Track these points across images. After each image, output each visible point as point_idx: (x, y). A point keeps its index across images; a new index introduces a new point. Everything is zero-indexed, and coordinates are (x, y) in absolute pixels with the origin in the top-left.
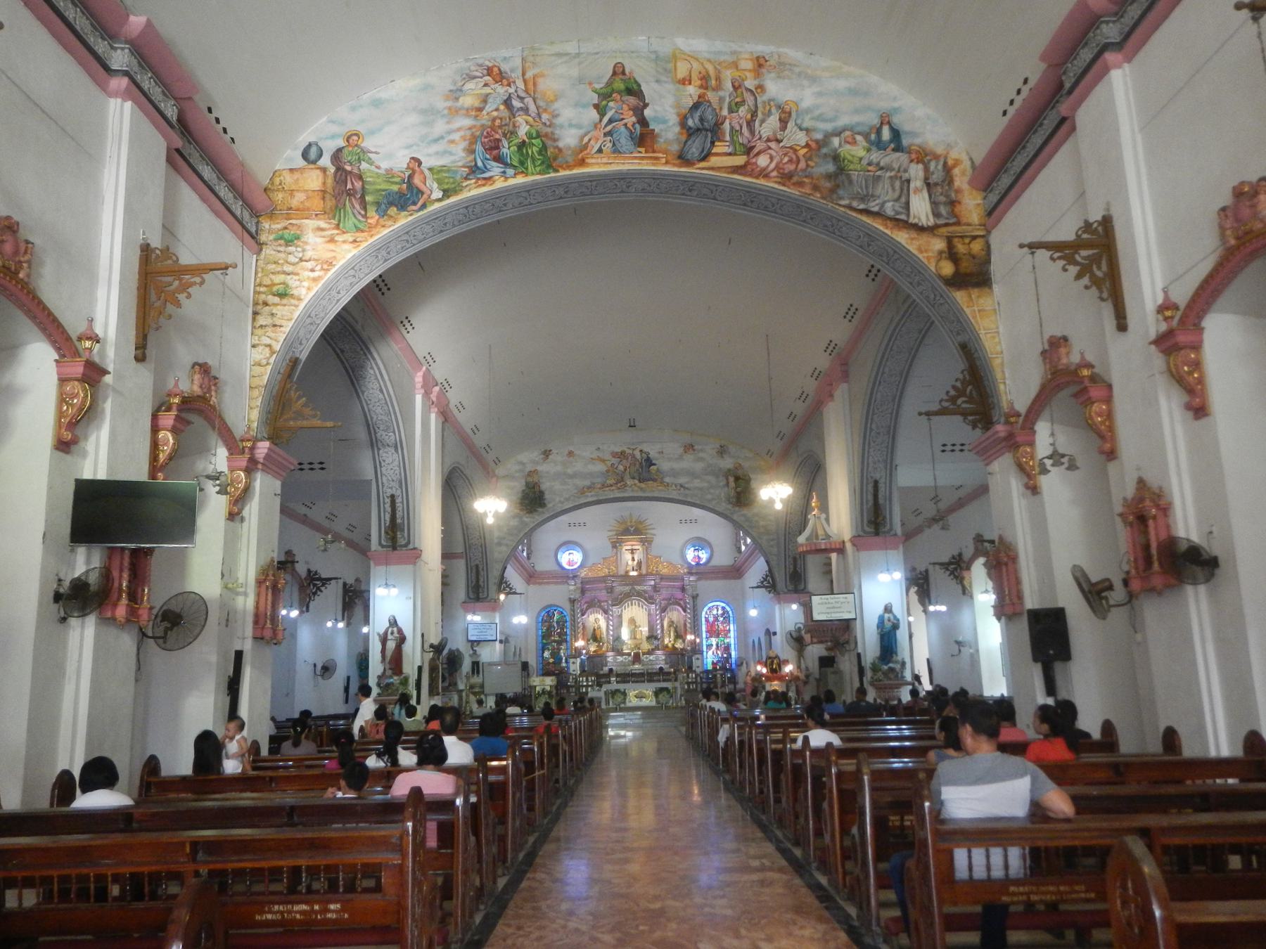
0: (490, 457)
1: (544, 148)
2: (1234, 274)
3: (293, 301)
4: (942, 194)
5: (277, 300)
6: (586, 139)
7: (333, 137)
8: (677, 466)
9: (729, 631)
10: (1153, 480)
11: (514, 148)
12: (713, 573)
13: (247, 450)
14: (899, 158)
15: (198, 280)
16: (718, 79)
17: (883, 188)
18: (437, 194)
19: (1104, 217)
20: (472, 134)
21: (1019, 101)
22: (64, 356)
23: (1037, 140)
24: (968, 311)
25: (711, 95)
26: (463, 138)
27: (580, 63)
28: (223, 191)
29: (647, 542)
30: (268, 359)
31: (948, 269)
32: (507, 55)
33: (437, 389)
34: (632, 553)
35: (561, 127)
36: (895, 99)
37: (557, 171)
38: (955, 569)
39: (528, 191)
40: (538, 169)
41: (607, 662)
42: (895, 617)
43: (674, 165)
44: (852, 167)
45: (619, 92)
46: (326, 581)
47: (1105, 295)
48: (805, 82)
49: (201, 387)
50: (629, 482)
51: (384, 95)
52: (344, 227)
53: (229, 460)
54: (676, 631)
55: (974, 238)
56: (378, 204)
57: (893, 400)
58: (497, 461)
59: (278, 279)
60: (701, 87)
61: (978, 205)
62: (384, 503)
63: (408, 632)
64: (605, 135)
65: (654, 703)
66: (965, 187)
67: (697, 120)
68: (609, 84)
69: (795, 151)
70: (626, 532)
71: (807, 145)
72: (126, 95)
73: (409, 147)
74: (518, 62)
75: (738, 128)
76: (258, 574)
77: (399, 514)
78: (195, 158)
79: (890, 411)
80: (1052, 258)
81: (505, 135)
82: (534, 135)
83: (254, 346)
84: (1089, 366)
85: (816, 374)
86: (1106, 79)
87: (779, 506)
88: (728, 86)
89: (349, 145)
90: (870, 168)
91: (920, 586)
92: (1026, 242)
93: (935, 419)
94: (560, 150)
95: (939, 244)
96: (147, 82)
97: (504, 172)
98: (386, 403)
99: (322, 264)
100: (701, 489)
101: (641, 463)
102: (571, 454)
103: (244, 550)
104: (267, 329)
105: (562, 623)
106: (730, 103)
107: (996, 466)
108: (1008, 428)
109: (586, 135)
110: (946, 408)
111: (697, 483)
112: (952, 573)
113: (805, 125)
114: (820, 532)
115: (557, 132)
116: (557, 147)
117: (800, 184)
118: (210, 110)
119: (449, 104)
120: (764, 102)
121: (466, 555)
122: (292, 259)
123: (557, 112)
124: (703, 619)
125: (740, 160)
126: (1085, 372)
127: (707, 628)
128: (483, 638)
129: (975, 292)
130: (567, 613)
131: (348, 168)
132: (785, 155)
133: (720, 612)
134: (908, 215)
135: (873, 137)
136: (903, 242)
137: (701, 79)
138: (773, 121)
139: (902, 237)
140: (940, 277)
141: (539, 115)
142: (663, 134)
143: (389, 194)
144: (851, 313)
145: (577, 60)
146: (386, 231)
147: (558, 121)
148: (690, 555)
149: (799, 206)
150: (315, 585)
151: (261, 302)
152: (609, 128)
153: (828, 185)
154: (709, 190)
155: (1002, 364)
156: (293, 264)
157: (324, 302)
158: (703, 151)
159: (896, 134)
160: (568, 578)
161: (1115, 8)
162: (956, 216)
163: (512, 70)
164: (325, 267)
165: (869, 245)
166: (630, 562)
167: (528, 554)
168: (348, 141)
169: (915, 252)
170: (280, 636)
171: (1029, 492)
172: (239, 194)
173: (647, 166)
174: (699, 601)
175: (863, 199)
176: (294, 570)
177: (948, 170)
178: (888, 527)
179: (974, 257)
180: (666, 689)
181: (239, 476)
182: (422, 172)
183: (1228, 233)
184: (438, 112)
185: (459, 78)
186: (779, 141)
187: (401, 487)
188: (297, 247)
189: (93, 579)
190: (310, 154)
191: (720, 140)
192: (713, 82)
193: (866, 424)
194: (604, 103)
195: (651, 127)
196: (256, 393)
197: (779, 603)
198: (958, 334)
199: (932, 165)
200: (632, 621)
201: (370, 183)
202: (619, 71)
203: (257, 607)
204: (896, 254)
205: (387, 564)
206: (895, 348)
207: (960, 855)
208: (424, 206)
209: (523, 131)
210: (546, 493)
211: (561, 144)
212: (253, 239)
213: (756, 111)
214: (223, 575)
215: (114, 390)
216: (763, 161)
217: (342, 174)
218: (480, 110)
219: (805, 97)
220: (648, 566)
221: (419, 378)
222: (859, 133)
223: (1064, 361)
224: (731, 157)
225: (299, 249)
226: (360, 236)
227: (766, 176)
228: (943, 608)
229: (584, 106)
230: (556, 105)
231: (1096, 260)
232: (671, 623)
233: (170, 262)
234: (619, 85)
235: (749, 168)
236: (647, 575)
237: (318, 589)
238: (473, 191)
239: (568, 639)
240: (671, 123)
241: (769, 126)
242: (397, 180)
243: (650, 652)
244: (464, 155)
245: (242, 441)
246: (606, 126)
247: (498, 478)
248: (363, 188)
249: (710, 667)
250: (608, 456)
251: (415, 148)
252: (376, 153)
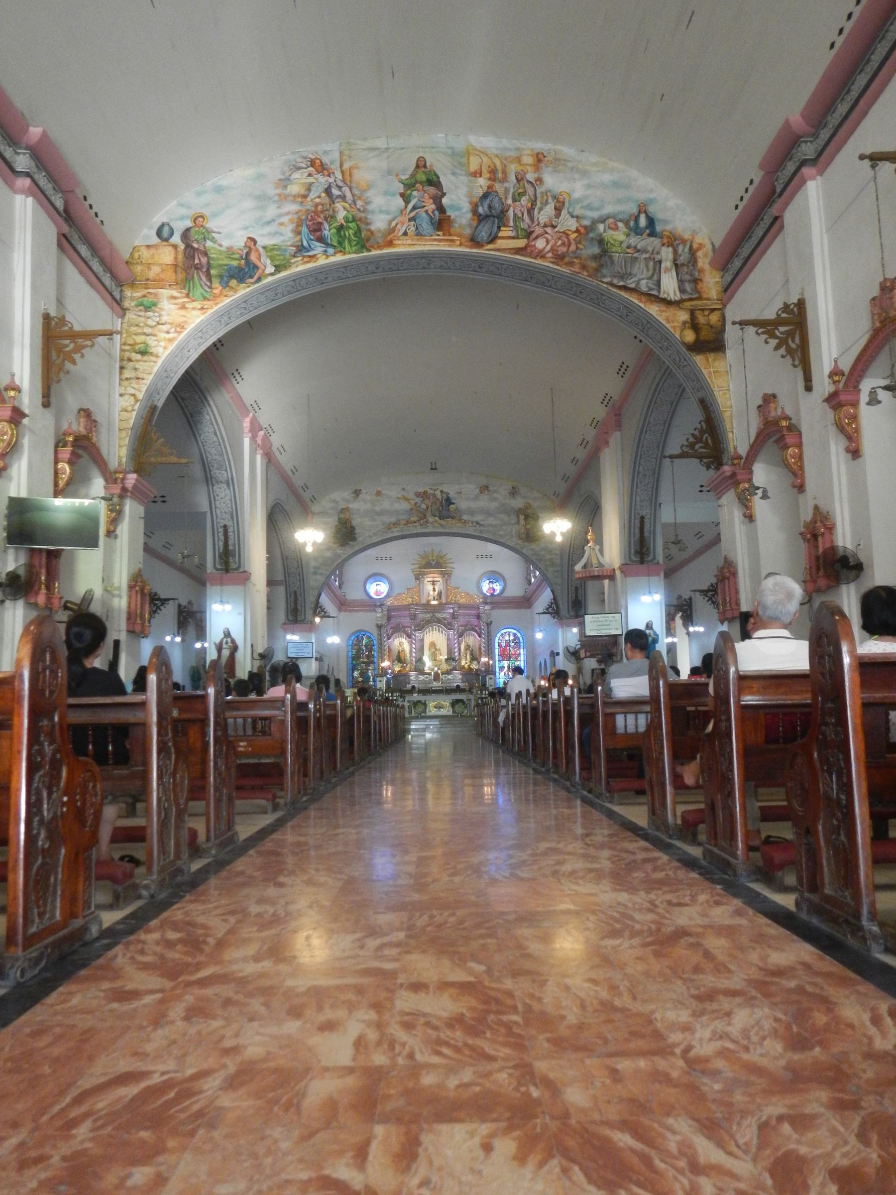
0: (306, 496)
1: (359, 231)
2: (880, 348)
3: (153, 358)
4: (687, 273)
5: (139, 357)
6: (394, 224)
7: (182, 218)
8: (473, 505)
9: (519, 654)
10: (823, 507)
11: (334, 231)
12: (506, 603)
13: (119, 481)
14: (653, 242)
15: (89, 343)
16: (504, 172)
17: (639, 268)
18: (270, 269)
19: (799, 300)
20: (299, 219)
21: (747, 197)
23: (759, 232)
24: (704, 371)
25: (498, 187)
26: (291, 221)
27: (388, 157)
28: (96, 265)
29: (447, 575)
30: (133, 406)
31: (690, 336)
32: (327, 148)
33: (261, 433)
34: (433, 584)
35: (373, 212)
36: (651, 191)
37: (370, 251)
38: (713, 595)
39: (345, 267)
40: (354, 249)
41: (410, 680)
42: (655, 633)
43: (467, 247)
44: (614, 249)
45: (421, 183)
46: (164, 601)
47: (797, 362)
48: (577, 176)
49: (85, 428)
50: (431, 519)
51: (224, 181)
53: (105, 488)
54: (472, 654)
55: (713, 310)
56: (221, 277)
57: (658, 446)
58: (313, 499)
60: (490, 179)
61: (717, 282)
63: (240, 642)
64: (410, 220)
65: (451, 713)
66: (707, 267)
67: (486, 206)
68: (413, 175)
69: (567, 235)
70: (428, 565)
71: (577, 231)
72: (28, 192)
73: (246, 228)
74: (336, 155)
75: (520, 215)
76: (130, 581)
77: (231, 542)
79: (655, 456)
80: (757, 333)
81: (326, 219)
82: (351, 219)
83: (121, 395)
84: (788, 418)
85: (595, 423)
86: (803, 188)
87: (559, 539)
88: (513, 178)
89: (196, 226)
90: (629, 251)
91: (684, 611)
92: (737, 320)
93: (676, 461)
94: (372, 233)
95: (684, 316)
96: (43, 182)
97: (325, 251)
98: (220, 445)
100: (494, 526)
101: (441, 503)
102: (379, 493)
103: (118, 560)
105: (370, 647)
106: (513, 193)
107: (724, 500)
108: (732, 468)
109: (393, 219)
110: (687, 452)
111: (491, 521)
112: (710, 599)
113: (575, 214)
114: (594, 561)
115: (369, 217)
116: (370, 230)
117: (571, 264)
118: (85, 198)
119: (278, 191)
120: (542, 193)
121: (286, 583)
123: (369, 200)
124: (497, 645)
125: (521, 243)
126: (784, 423)
127: (500, 652)
128: (300, 655)
129: (711, 356)
130: (375, 638)
131: (195, 245)
132: (559, 238)
133: (512, 638)
134: (659, 291)
135: (632, 223)
136: (654, 314)
137: (490, 172)
138: (549, 209)
139: (653, 310)
140: (684, 343)
141: (354, 202)
142: (458, 219)
143: (230, 268)
144: (623, 370)
145: (386, 155)
146: (228, 300)
147: (370, 207)
148: (486, 586)
149: (570, 282)
150: (155, 605)
151: (126, 358)
152: (412, 214)
153: (593, 264)
154: (496, 267)
155: (731, 416)
157: (177, 359)
158: (491, 234)
159: (651, 221)
160: (375, 606)
161: (813, 130)
162: (698, 292)
163: (332, 162)
164: (178, 329)
165: (627, 316)
166: (431, 593)
167: (340, 584)
168: (195, 221)
169: (664, 322)
170: (146, 632)
171: (747, 520)
172: (108, 269)
173: (444, 247)
174: (493, 627)
175: (622, 277)
177: (693, 252)
178: (651, 556)
179: (712, 327)
180: (462, 701)
182: (257, 250)
183: (876, 317)
184: (270, 198)
185: (286, 169)
186: (554, 227)
187: (232, 518)
188: (155, 312)
189: (22, 572)
190: (163, 233)
191: (505, 226)
192: (500, 175)
193: (635, 467)
194: (409, 192)
195: (448, 214)
196: (124, 434)
197: (562, 625)
198: (698, 391)
199: (680, 248)
200: (433, 645)
201: (213, 259)
202: (421, 164)
203: (129, 607)
204: (647, 324)
205: (221, 584)
206: (658, 401)
207: (620, 720)
208: (259, 280)
209: (341, 215)
210: (357, 528)
211: (373, 228)
212: (118, 305)
213: (535, 201)
214: (103, 580)
215: (30, 430)
216: (540, 244)
217: (190, 251)
218: (305, 197)
219: (577, 189)
220: (447, 597)
221: (246, 423)
222: (620, 221)
223: (773, 414)
224: (511, 241)
225: (156, 314)
226: (207, 304)
227: (543, 257)
228: (701, 629)
229: (393, 195)
230: (369, 194)
231: (790, 334)
232: (468, 647)
233: (66, 328)
234: (421, 177)
235: (529, 250)
236: (446, 604)
237: (158, 608)
238: (299, 267)
239: (376, 660)
240: (464, 211)
241: (546, 214)
242: (237, 256)
243: (448, 672)
244: (290, 235)
245: (115, 472)
246: (411, 212)
247: (314, 514)
248: (208, 262)
249: (501, 685)
250: (412, 496)
251: (251, 229)
252: (219, 233)
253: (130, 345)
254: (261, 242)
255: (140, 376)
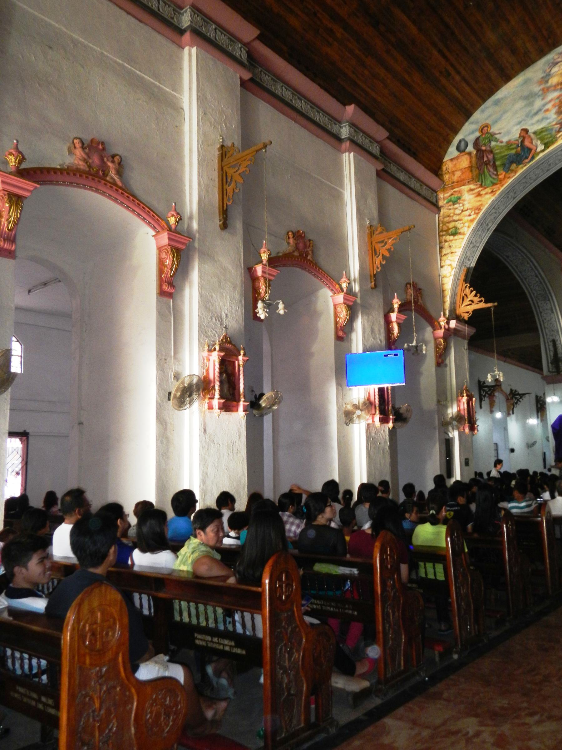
3: (461, 236)
5: (452, 237)
7: (473, 132)
18: (541, 147)
22: (335, 293)
26: (554, 106)
46: (522, 396)
52: (485, 185)
56: (504, 165)
59: (451, 225)
62: (549, 345)
78: (393, 169)
96: (360, 139)
98: (541, 283)
99: (475, 210)
104: (448, 255)
119: (542, 87)
122: (458, 212)
131: (484, 148)
143: (510, 156)
150: (516, 398)
151: (443, 241)
156: (459, 214)
164: (477, 211)
168: (482, 131)
176: (502, 390)
181: (440, 341)
182: (530, 137)
184: (536, 94)
185: (546, 67)
188: (459, 204)
201: (497, 154)
208: (533, 158)
225: (461, 205)
226: (495, 188)
237: (518, 400)
242: (514, 146)
248: (494, 158)
251: (523, 122)
252: (500, 133)
253: (445, 231)
254: (532, 129)
255: (453, 251)
